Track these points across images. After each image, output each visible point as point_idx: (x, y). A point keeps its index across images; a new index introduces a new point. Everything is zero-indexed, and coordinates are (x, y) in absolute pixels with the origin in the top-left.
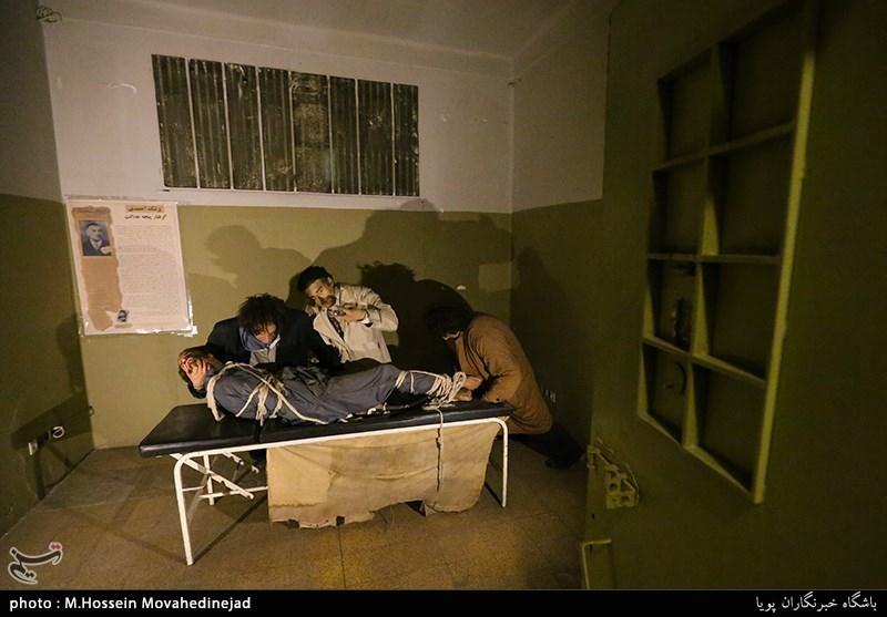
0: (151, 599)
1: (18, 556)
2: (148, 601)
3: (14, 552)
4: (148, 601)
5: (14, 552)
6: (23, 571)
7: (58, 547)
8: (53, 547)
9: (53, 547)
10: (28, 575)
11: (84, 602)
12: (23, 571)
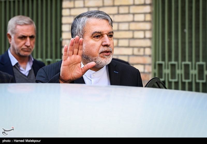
0: (28, 140)
1: (4, 130)
2: (27, 140)
3: (3, 129)
4: (27, 140)
5: (3, 129)
6: (5, 133)
7: (13, 128)
8: (12, 128)
9: (12, 128)
10: (6, 134)
11: (14, 141)
12: (5, 133)
